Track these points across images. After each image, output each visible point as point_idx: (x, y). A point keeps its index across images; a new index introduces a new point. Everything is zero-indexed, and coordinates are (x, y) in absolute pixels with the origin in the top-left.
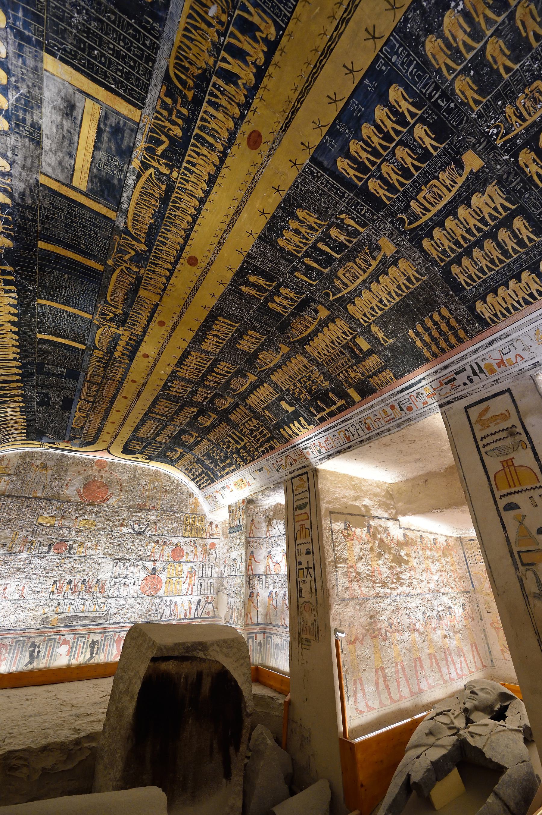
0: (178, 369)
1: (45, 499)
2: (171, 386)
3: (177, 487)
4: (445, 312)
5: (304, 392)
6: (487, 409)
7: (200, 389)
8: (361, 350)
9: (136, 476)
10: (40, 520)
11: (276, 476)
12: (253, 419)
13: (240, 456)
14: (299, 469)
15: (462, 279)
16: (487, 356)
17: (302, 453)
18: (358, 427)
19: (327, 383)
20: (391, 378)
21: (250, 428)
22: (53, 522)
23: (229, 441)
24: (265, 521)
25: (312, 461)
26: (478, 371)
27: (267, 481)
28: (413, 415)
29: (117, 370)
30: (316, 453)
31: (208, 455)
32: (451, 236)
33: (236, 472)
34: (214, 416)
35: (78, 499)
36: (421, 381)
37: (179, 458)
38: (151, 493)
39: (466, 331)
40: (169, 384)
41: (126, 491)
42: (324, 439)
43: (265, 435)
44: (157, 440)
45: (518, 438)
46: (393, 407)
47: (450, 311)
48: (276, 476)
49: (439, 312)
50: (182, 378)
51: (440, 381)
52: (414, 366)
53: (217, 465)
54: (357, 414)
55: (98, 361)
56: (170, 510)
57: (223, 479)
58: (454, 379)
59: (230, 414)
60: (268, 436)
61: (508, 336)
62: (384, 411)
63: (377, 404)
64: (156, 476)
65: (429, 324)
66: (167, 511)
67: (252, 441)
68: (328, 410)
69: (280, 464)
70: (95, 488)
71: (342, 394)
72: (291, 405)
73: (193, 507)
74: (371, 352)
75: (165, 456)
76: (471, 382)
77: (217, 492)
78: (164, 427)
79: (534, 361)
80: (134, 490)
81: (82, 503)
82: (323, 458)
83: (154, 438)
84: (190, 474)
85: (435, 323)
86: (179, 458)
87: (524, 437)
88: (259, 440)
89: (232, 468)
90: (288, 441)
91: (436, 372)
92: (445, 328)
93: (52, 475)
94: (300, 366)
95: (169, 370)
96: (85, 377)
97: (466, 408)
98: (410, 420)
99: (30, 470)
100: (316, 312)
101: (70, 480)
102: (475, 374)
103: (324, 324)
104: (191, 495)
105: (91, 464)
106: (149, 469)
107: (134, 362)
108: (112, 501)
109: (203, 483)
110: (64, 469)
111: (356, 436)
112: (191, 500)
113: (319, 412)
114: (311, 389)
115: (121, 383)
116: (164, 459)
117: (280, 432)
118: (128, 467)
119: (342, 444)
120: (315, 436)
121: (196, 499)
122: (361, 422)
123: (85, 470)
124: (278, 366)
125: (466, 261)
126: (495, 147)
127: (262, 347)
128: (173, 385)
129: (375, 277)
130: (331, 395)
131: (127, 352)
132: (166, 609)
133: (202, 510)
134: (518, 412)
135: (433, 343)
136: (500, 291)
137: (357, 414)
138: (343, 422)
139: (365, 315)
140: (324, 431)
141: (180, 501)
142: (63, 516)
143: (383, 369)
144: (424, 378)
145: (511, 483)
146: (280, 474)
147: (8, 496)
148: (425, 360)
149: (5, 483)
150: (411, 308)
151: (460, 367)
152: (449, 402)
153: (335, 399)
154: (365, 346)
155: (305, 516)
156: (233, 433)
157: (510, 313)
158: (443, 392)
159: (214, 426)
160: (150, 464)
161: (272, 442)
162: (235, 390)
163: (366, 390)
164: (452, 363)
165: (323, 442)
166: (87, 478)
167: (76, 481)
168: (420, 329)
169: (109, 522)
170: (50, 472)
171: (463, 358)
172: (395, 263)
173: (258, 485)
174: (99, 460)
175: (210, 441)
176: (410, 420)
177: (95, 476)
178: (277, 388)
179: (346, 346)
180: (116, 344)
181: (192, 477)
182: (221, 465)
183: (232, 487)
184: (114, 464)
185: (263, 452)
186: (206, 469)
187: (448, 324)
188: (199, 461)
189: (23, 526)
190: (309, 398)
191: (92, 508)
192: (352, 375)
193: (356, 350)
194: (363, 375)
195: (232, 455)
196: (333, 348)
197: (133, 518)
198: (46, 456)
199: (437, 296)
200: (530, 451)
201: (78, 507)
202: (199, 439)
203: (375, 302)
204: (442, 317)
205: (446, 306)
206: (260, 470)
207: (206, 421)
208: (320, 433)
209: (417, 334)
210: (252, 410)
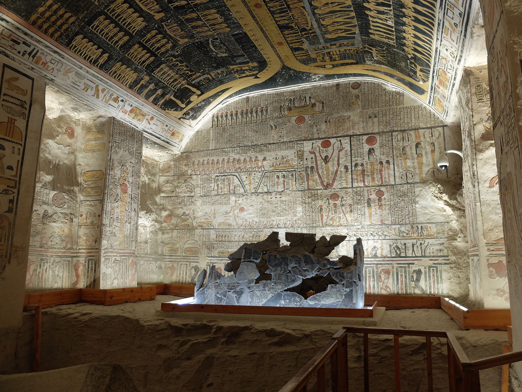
4: (72, 19)
6: (17, 79)
15: (96, 23)
16: (46, 54)
26: (33, 54)
32: (123, 12)
39: (60, 36)
45: (24, 111)
51: (11, 35)
52: (17, 11)
58: (19, 44)
61: (63, 58)
65: (60, 12)
76: (23, 55)
79: (53, 78)
85: (61, 16)
87: (27, 112)
91: (18, 29)
92: (59, 23)
97: (5, 65)
125: (107, 22)
126: (162, 22)
134: (32, 97)
135: (45, 19)
136: (91, 43)
144: (7, 22)
145: (8, 133)
148: (26, 18)
151: (30, 43)
157: (88, 60)
164: (32, 37)
168: (55, 7)
171: (39, 42)
187: (62, 24)
199: (83, 12)
200: (26, 121)
204: (67, 19)
205: (76, 19)
209: (50, 6)
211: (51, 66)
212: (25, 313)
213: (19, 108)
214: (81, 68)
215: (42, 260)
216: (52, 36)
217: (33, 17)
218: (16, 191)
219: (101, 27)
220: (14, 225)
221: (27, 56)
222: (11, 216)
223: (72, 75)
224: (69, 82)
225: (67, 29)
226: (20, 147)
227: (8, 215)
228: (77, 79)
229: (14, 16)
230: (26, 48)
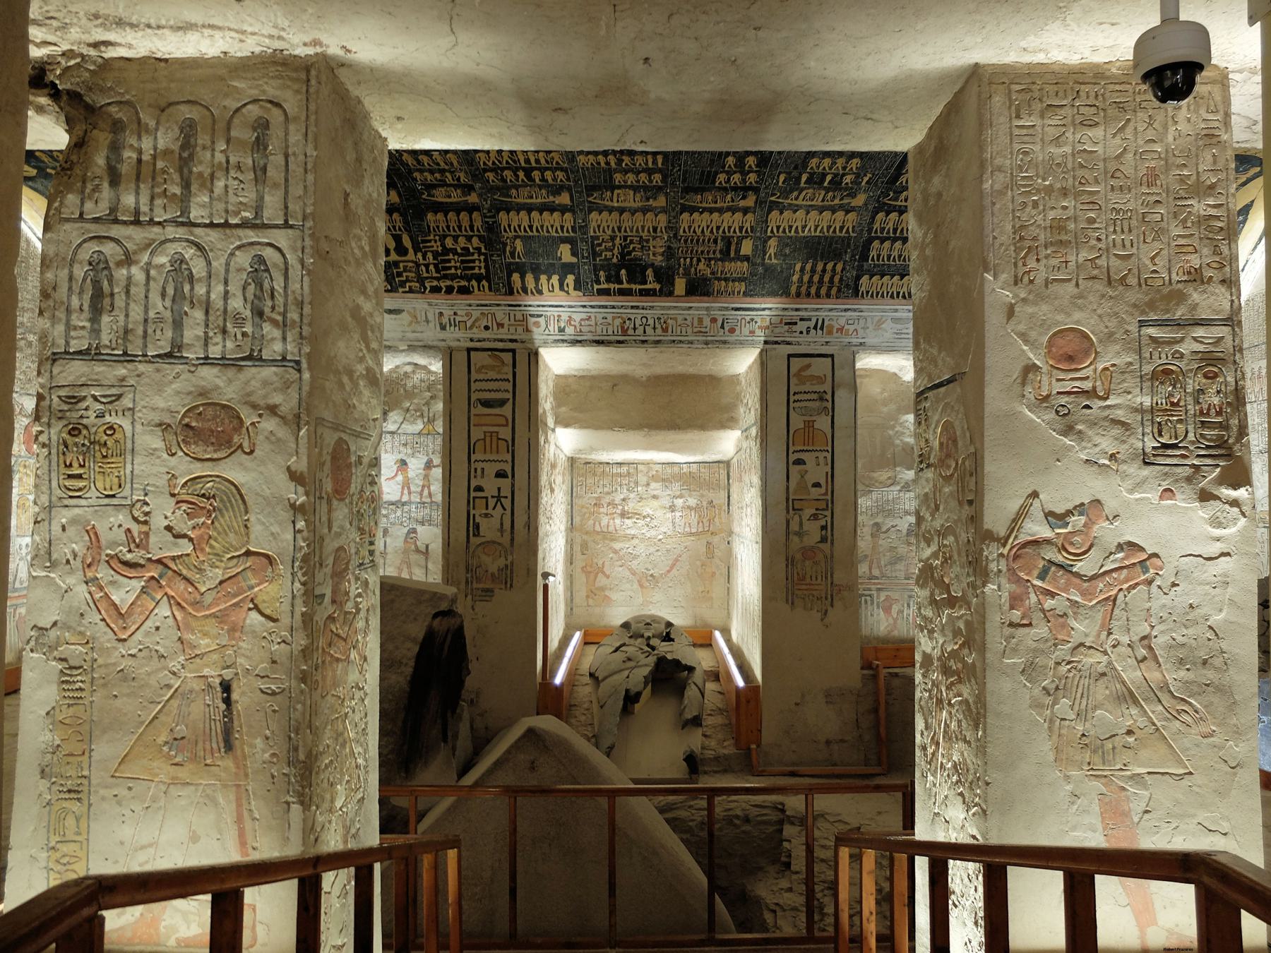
4: (839, 267)
5: (616, 251)
6: (809, 366)
8: (738, 250)
11: (431, 333)
12: (475, 240)
14: (501, 340)
15: (873, 253)
17: (525, 318)
18: (651, 322)
19: (660, 258)
20: (739, 292)
25: (536, 337)
26: (819, 326)
27: (400, 335)
28: (731, 338)
30: (553, 328)
36: (765, 309)
39: (839, 290)
42: (584, 316)
43: (473, 268)
45: (825, 404)
46: (714, 320)
47: (843, 269)
48: (431, 333)
49: (835, 265)
52: (773, 294)
54: (663, 308)
60: (476, 271)
62: (700, 320)
63: (698, 309)
65: (820, 267)
68: (625, 286)
69: (458, 319)
71: (665, 278)
72: (574, 254)
74: (747, 258)
82: (563, 341)
85: (824, 271)
87: (829, 405)
88: (450, 268)
90: (511, 292)
92: (826, 279)
94: (649, 225)
97: (789, 356)
98: (725, 342)
100: (744, 198)
102: (815, 328)
103: (733, 210)
111: (640, 330)
113: (608, 280)
114: (629, 253)
117: (509, 276)
119: (610, 332)
120: (570, 307)
122: (659, 319)
124: (622, 211)
125: (887, 244)
127: (635, 189)
129: (821, 210)
130: (649, 272)
132: (21, 564)
136: (886, 278)
137: (660, 307)
138: (632, 307)
139: (778, 228)
140: (592, 307)
143: (740, 280)
146: (442, 335)
148: (786, 293)
150: (821, 249)
152: (776, 343)
153: (651, 278)
154: (747, 248)
155: (503, 421)
158: (777, 330)
161: (474, 283)
163: (698, 288)
165: (578, 319)
168: (808, 267)
171: (817, 310)
172: (847, 212)
176: (725, 342)
178: (584, 228)
179: (728, 241)
185: (436, 290)
190: (615, 260)
192: (701, 266)
193: (733, 248)
194: (712, 273)
196: (712, 232)
200: (829, 418)
203: (799, 224)
204: (834, 269)
208: (584, 306)
209: (802, 270)
211: (851, 328)
212: (865, 672)
213: (818, 403)
214: (896, 311)
215: (910, 597)
216: (828, 295)
217: (793, 289)
218: (828, 513)
219: (884, 253)
220: (832, 557)
221: (813, 331)
222: (826, 547)
223: (888, 325)
224: (888, 335)
225: (841, 280)
226: (825, 454)
227: (820, 545)
228: (899, 326)
229: (773, 300)
230: (806, 324)
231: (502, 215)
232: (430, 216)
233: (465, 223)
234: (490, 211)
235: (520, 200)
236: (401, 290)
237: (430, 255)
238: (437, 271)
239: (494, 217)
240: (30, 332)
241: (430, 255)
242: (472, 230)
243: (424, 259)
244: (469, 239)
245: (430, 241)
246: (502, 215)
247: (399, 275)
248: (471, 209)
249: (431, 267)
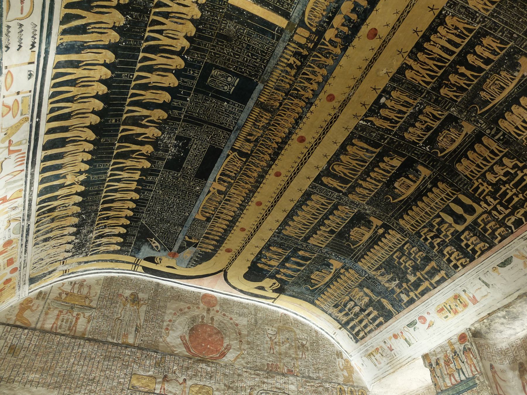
0: (411, 62)
1: (139, 348)
2: (384, 106)
3: (316, 343)
7: (428, 109)
9: (260, 321)
10: (134, 382)
12: (506, 161)
13: (459, 248)
21: (494, 180)
22: (152, 386)
23: (443, 222)
24: (513, 369)
29: (314, 73)
31: (389, 266)
33: (446, 283)
34: (425, 172)
35: (182, 350)
37: (327, 285)
38: (283, 348)
40: (383, 100)
41: (248, 343)
44: (312, 241)
50: (410, 83)
53: (403, 279)
55: (296, 54)
56: (314, 376)
57: (412, 307)
59: (459, 161)
64: (285, 324)
66: (309, 377)
67: (495, 209)
70: (206, 336)
73: (346, 374)
75: (307, 280)
77: (395, 336)
78: (336, 207)
80: (259, 343)
81: (190, 358)
83: (306, 239)
84: (340, 315)
86: (327, 285)
88: (511, 199)
89: (437, 278)
93: (147, 312)
95: (396, 65)
96: (261, 93)
99: (117, 303)
101: (170, 321)
104: (339, 354)
105: (196, 300)
106: (274, 312)
107: (350, 49)
108: (230, 357)
109: (366, 326)
110: (161, 304)
112: (340, 362)
115: (310, 103)
116: (303, 289)
118: (245, 307)
121: (347, 361)
123: (189, 308)
128: (389, 104)
131: (345, 29)
133: (360, 379)
141: (326, 363)
142: (165, 377)
147: (89, 340)
149: (86, 320)
156: (458, 202)
159: (419, 195)
160: (277, 303)
162: (487, 102)
166: (194, 319)
167: (180, 324)
169: (231, 391)
170: (144, 308)
173: (499, 296)
174: (205, 295)
175: (401, 230)
177: (203, 318)
180: (336, 11)
181: (345, 319)
182: (412, 279)
183: (433, 317)
184: (225, 302)
185: (518, 223)
186: (379, 294)
188: (368, 282)
189: (111, 389)
191: (204, 366)
195: (441, 252)
197: (265, 387)
198: (137, 284)
201: (186, 364)
202: (381, 231)
206: (503, 264)
207: (409, 186)
210: (507, 140)
231: (502, 123)
232: (459, 168)
233: (486, 154)
234: (491, 129)
235: (499, 99)
236: (496, 241)
237: (489, 199)
238: (506, 208)
239: (498, 131)
240: (326, 382)
241: (489, 199)
242: (497, 155)
243: (489, 205)
244: (500, 163)
245: (478, 188)
246: (502, 123)
247: (486, 230)
248: (478, 137)
249: (499, 207)
